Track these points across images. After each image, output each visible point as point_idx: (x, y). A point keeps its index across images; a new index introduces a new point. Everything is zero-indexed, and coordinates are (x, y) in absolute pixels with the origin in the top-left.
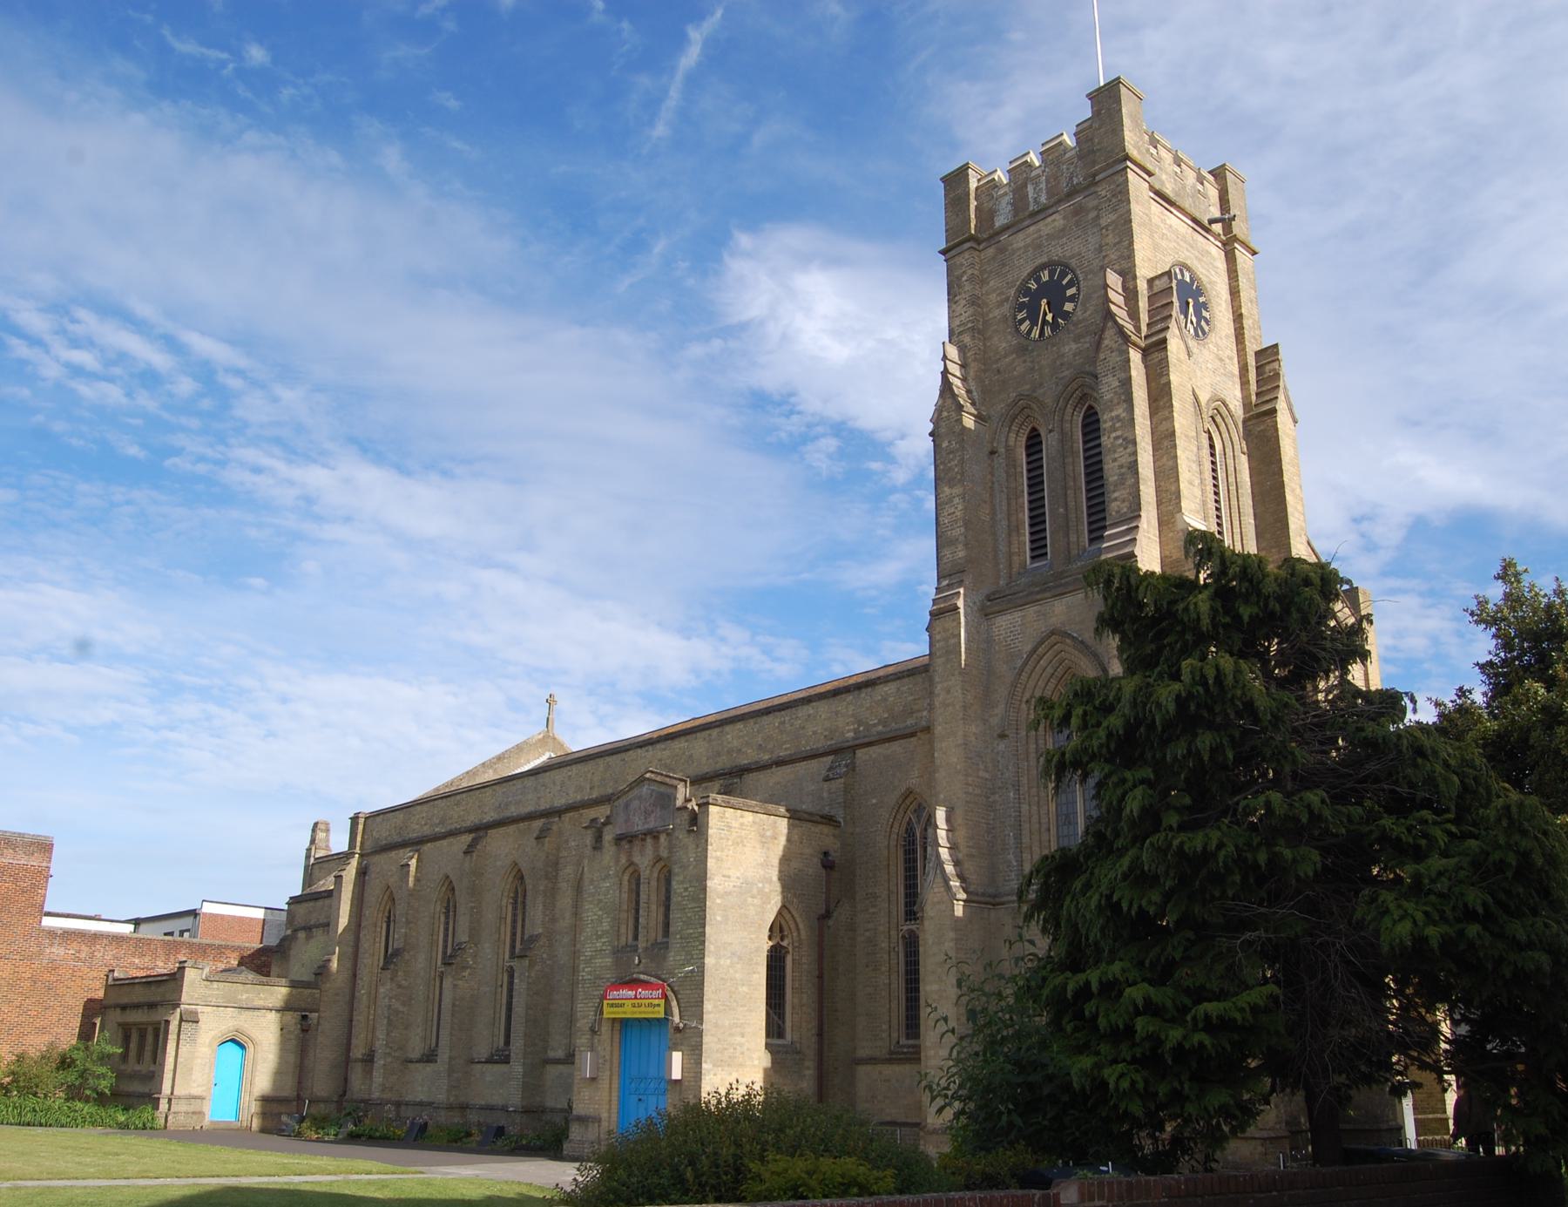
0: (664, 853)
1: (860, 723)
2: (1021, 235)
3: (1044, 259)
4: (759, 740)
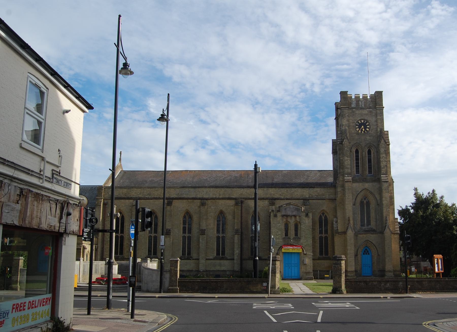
0: (299, 220)
1: (310, 195)
2: (358, 111)
3: (363, 118)
4: (280, 193)
